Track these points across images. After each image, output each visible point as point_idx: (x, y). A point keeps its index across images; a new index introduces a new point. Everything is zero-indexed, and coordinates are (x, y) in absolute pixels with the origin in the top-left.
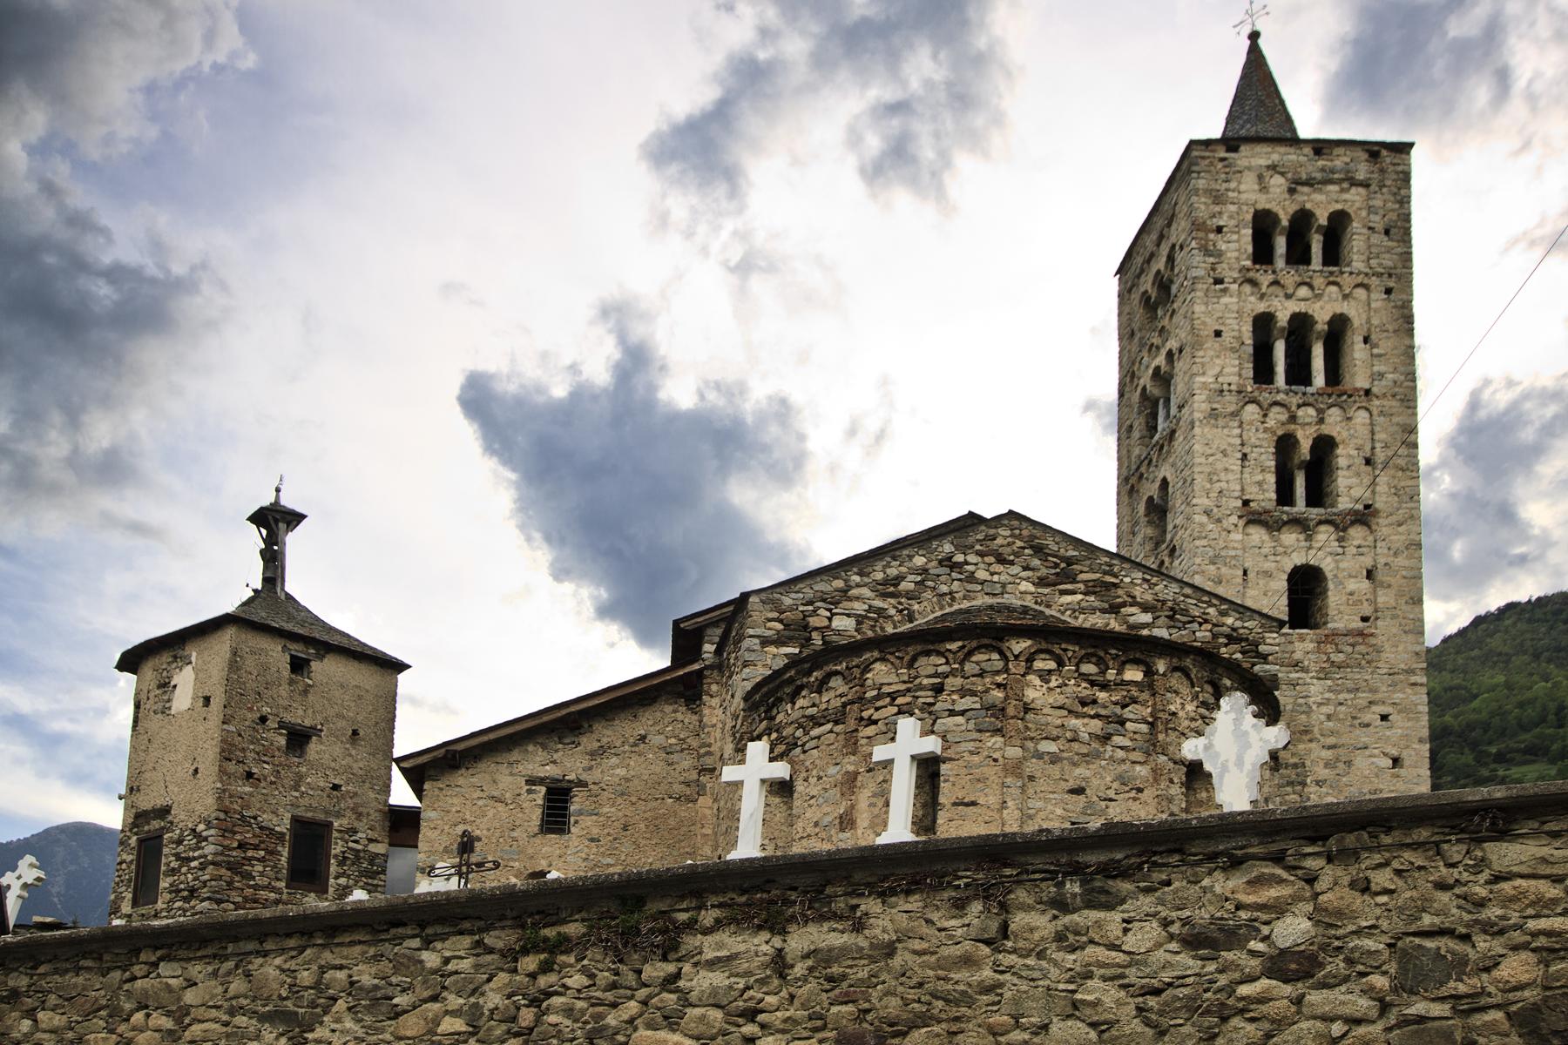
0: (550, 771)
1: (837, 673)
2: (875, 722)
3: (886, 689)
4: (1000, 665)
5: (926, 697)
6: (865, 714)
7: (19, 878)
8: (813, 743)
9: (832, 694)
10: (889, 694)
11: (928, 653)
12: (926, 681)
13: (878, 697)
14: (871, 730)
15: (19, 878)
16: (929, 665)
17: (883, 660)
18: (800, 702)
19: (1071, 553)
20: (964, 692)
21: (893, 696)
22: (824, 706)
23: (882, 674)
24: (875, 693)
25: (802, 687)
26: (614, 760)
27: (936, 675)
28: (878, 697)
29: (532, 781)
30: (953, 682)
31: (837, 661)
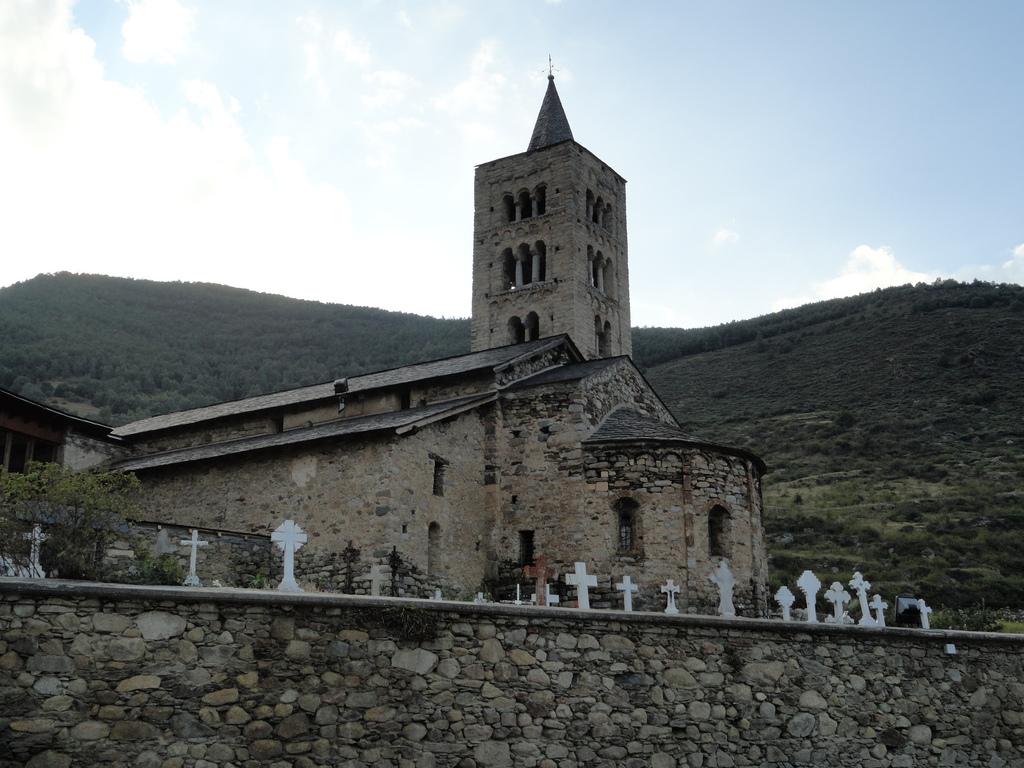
0: (436, 450)
1: (675, 454)
2: (699, 488)
3: (702, 472)
4: (743, 473)
5: (721, 482)
6: (694, 482)
7: (861, 584)
8: (660, 489)
9: (669, 465)
10: (705, 475)
11: (719, 458)
12: (721, 473)
13: (700, 475)
14: (696, 492)
15: (861, 584)
16: (721, 464)
17: (701, 455)
18: (641, 462)
19: (642, 386)
20: (736, 484)
21: (706, 476)
22: (664, 470)
23: (698, 461)
24: (697, 472)
25: (643, 453)
26: (457, 449)
27: (723, 471)
28: (700, 475)
29: (431, 456)
30: (730, 477)
31: (675, 447)
